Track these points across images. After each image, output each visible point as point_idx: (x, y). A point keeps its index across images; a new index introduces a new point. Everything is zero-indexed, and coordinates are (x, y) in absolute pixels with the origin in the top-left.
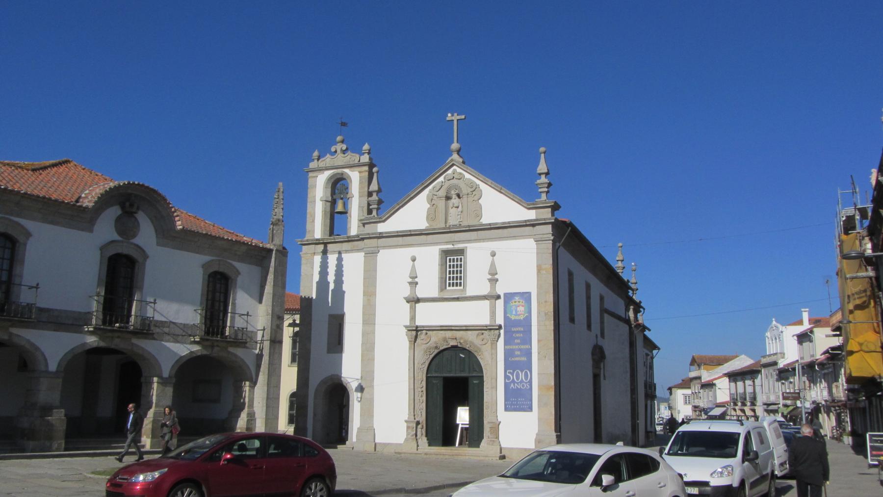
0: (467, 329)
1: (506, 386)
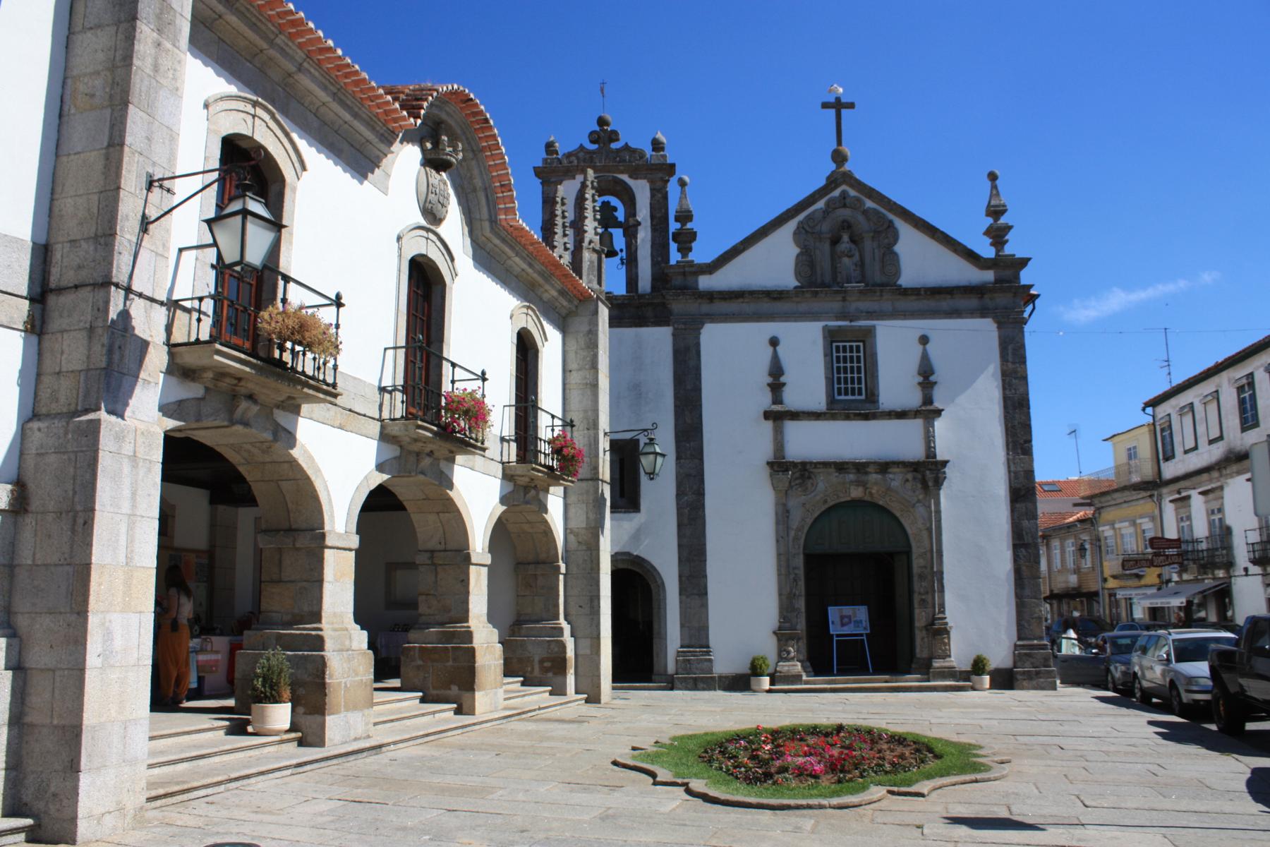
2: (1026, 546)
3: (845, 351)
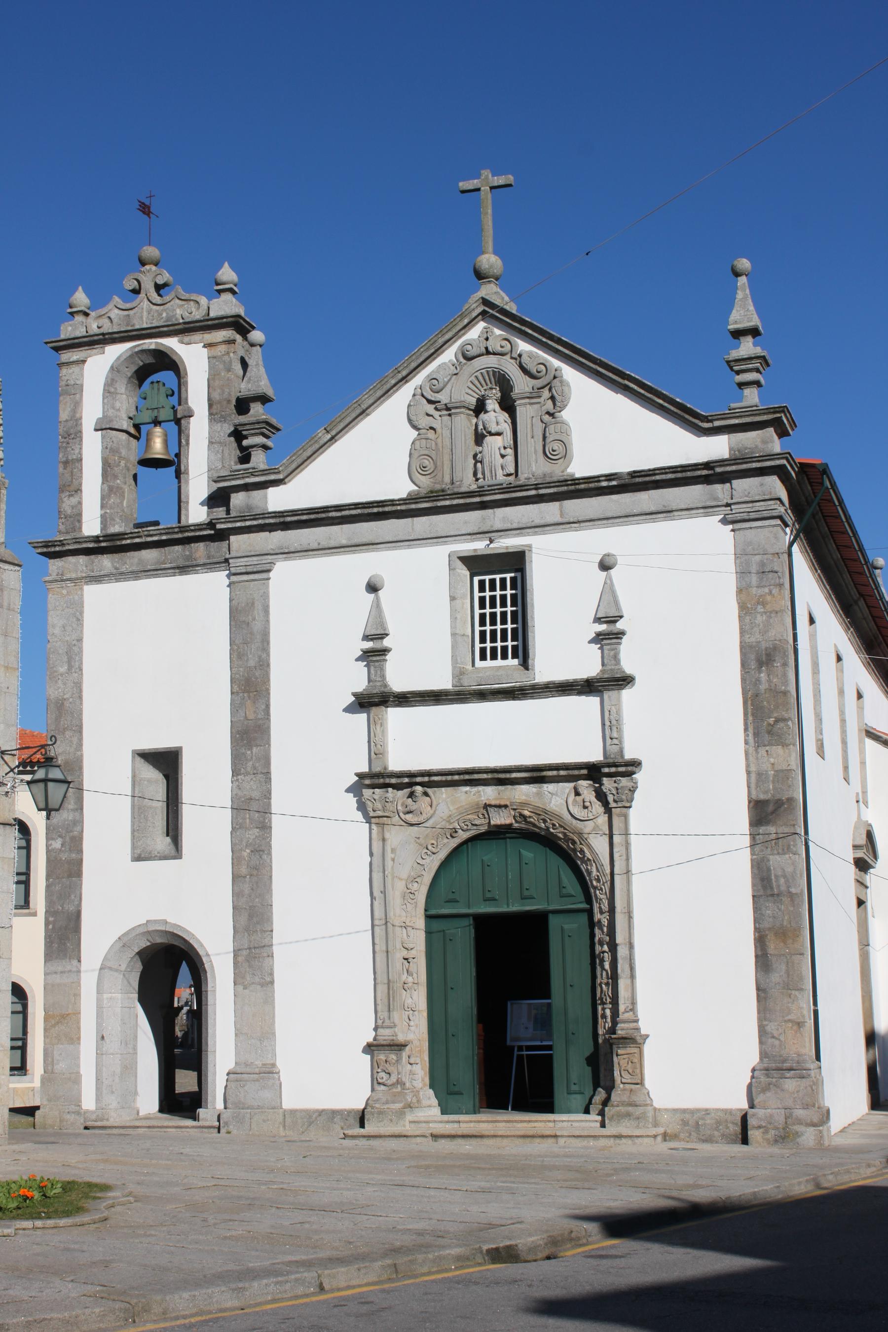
0: (537, 775)
2: (775, 896)
3: (493, 588)
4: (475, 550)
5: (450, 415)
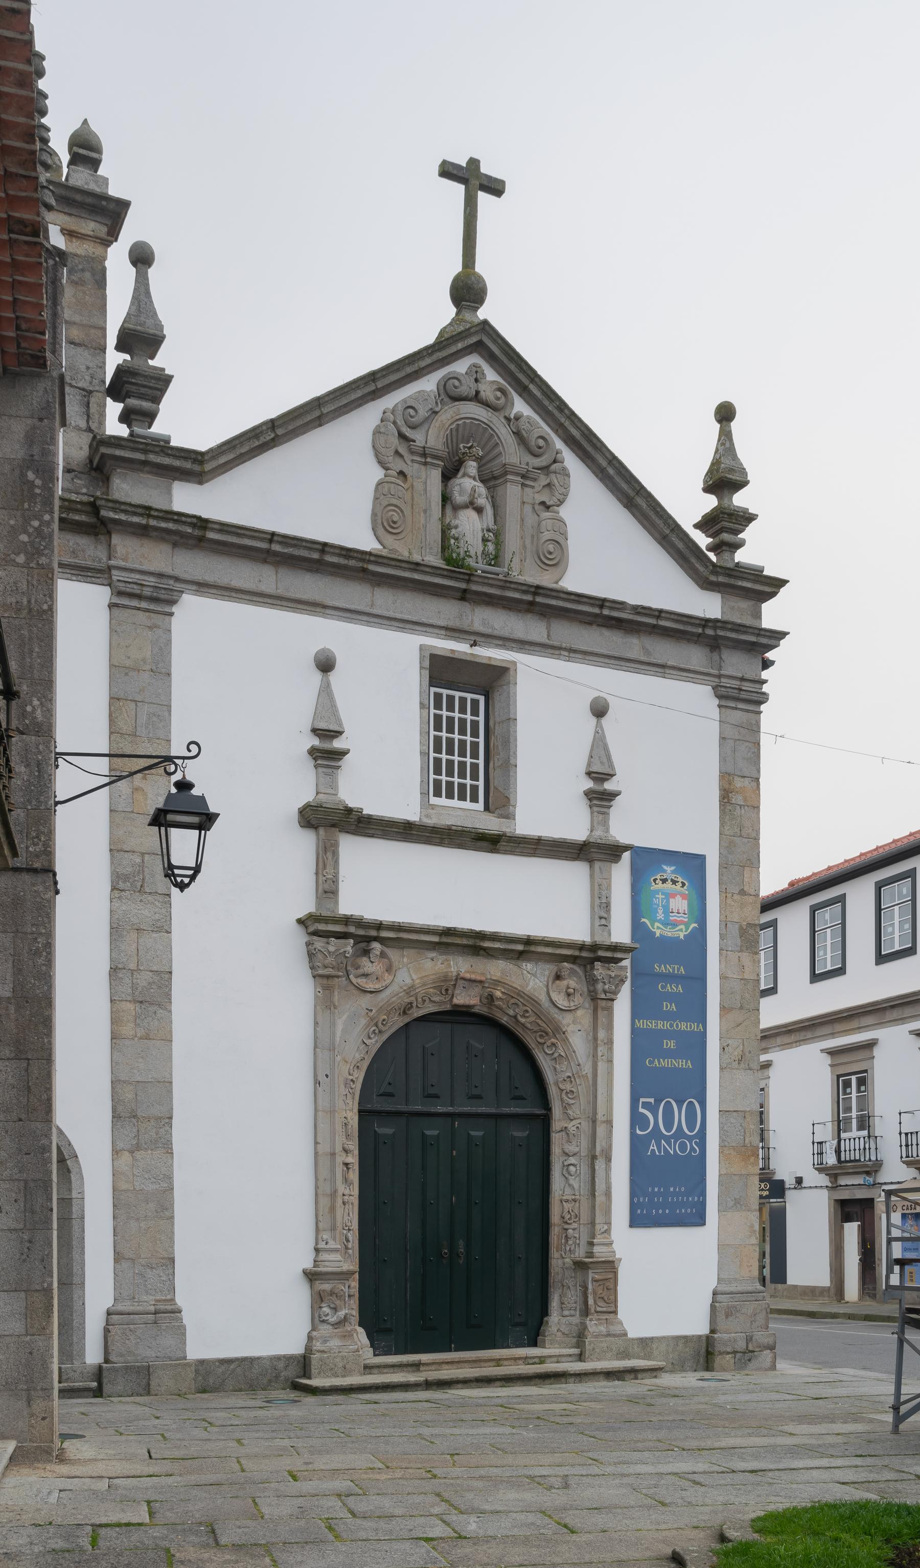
0: (524, 949)
1: (637, 1146)
4: (453, 651)
5: (523, 485)
